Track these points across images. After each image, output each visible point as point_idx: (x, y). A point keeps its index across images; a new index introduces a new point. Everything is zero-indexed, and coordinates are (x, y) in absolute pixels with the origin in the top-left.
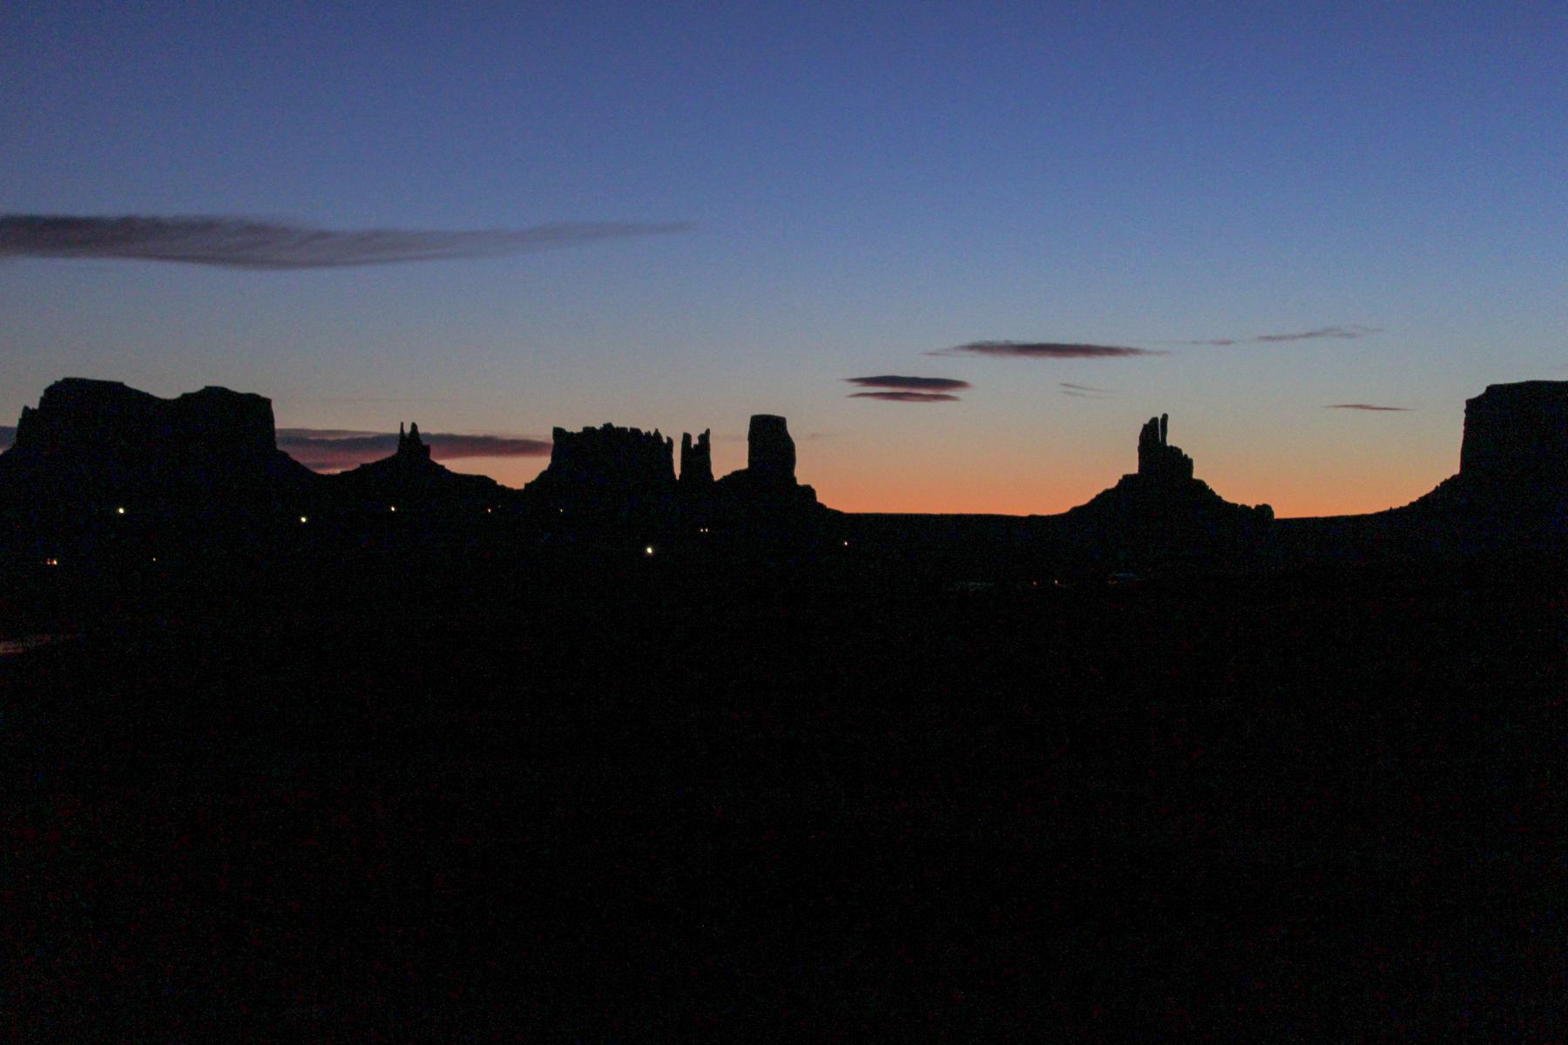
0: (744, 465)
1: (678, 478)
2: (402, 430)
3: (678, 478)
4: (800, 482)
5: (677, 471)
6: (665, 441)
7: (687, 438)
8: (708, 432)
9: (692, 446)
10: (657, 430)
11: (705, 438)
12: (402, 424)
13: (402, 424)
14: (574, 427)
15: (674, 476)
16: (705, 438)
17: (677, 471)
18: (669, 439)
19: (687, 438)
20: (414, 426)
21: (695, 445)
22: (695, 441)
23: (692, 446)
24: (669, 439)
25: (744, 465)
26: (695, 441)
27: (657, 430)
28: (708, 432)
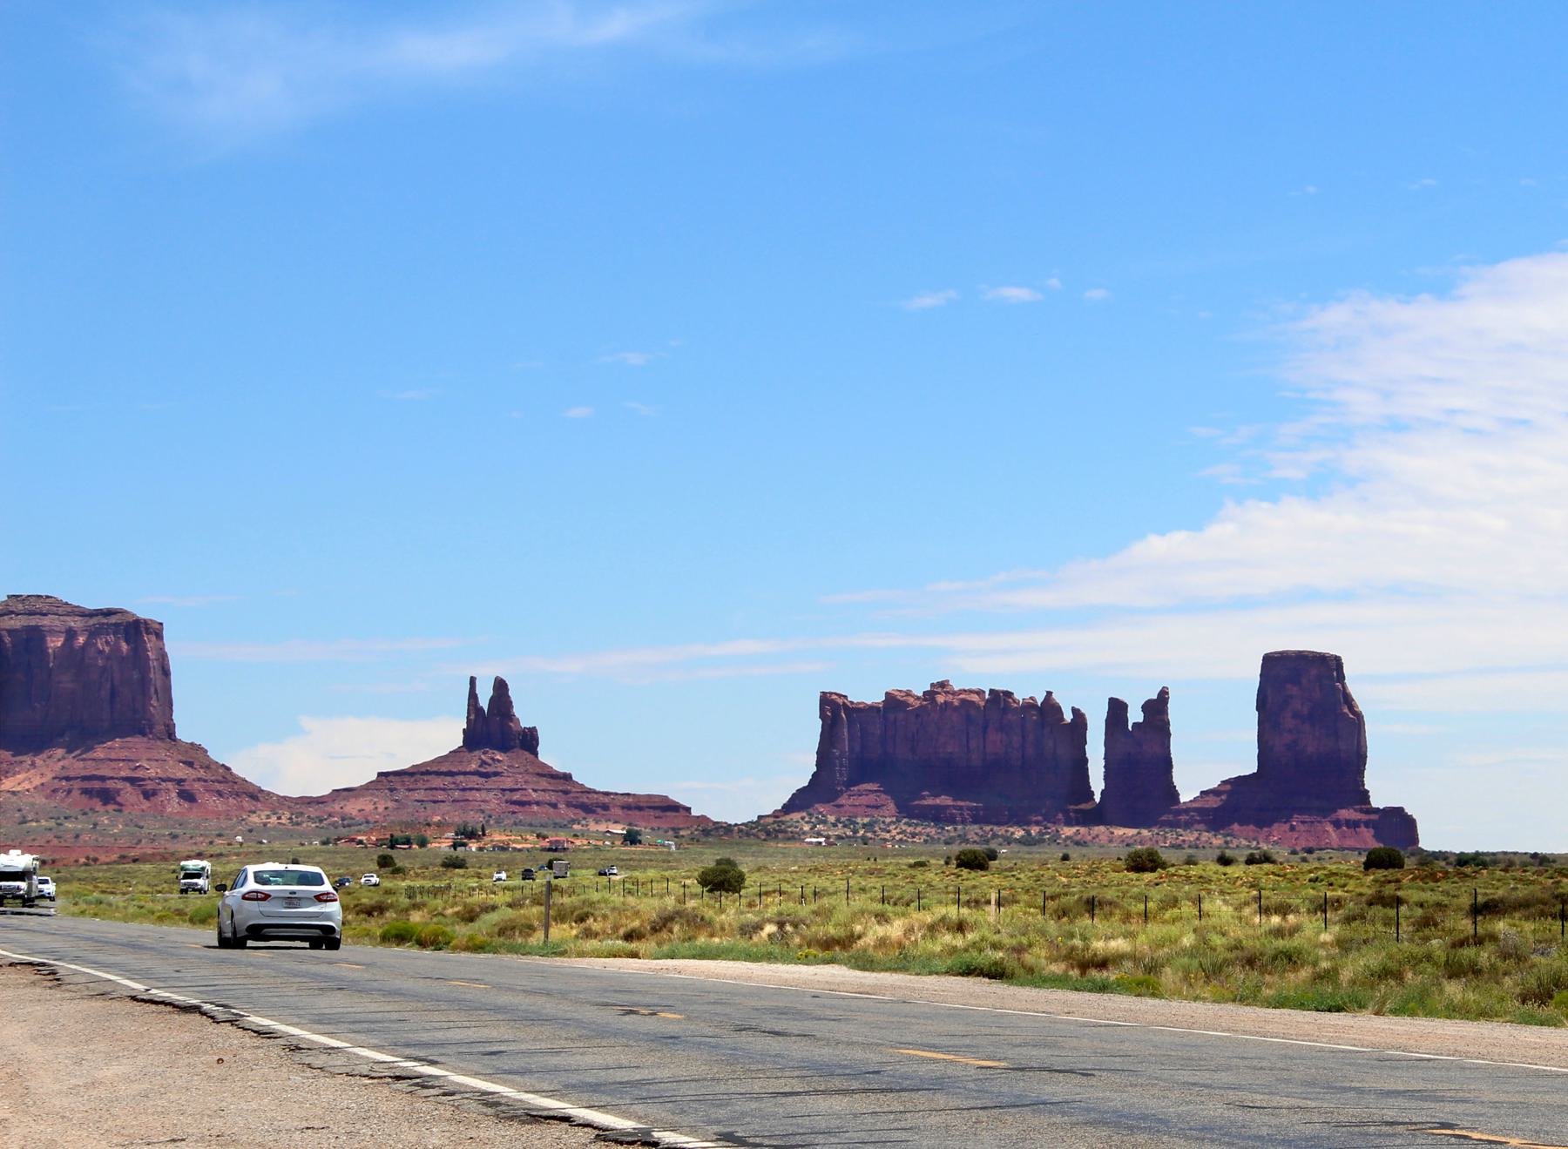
0: (1249, 766)
1: (1097, 798)
2: (473, 696)
3: (1097, 798)
4: (1380, 797)
5: (1097, 783)
6: (1068, 717)
7: (1117, 709)
8: (1163, 695)
9: (1130, 728)
10: (1049, 694)
11: (1157, 708)
12: (473, 681)
13: (473, 681)
14: (867, 693)
15: (1093, 793)
16: (1157, 708)
17: (1097, 783)
18: (1075, 711)
19: (1117, 709)
20: (501, 686)
21: (1135, 724)
22: (1135, 716)
23: (1130, 728)
24: (1075, 711)
25: (1249, 766)
26: (1135, 716)
27: (1049, 694)
28: (1163, 695)
